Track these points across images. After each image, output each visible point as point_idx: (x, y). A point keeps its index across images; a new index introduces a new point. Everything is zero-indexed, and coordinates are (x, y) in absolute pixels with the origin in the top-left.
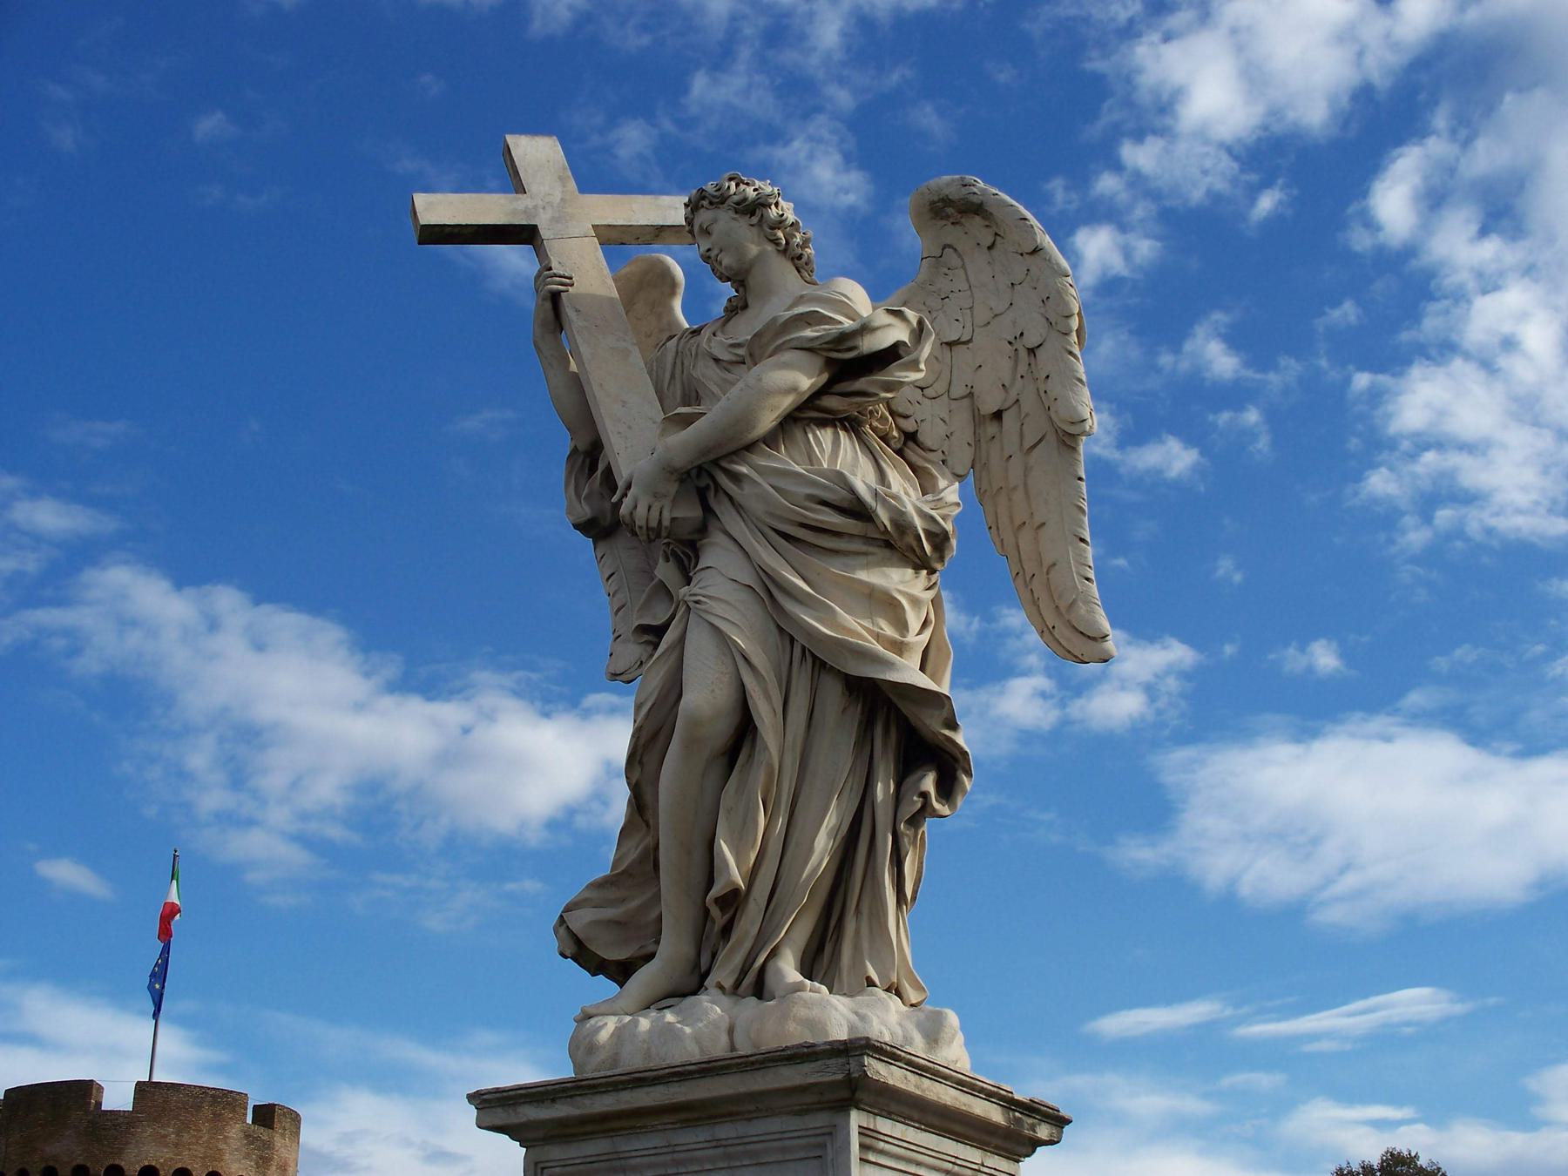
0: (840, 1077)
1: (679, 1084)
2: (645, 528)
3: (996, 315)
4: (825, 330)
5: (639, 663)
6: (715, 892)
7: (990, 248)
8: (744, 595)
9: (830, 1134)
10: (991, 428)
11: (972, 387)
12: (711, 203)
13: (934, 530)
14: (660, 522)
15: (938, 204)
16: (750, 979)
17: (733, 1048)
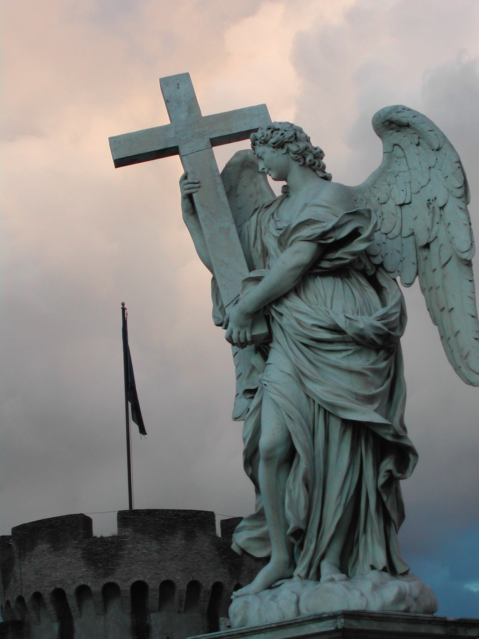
0: (333, 628)
5: (247, 410)
6: (289, 531)
10: (425, 253)
11: (413, 230)
12: (260, 143)
15: (386, 123)
17: (298, 612)
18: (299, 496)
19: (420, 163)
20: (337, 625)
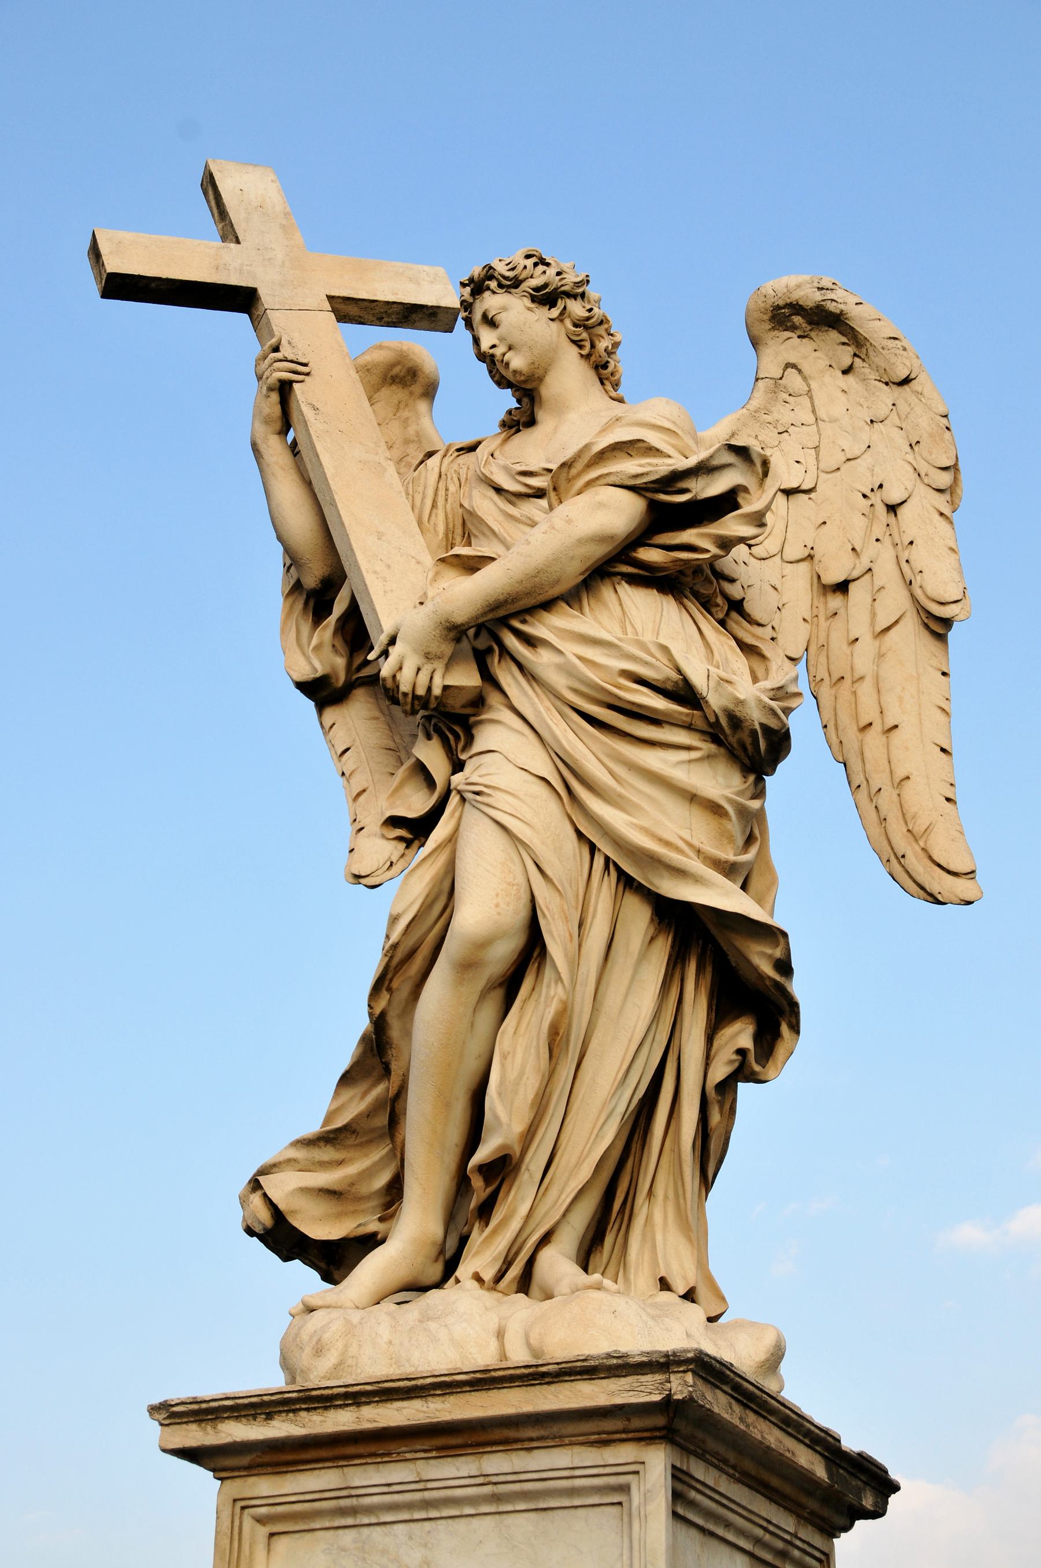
0: (657, 1398)
1: (441, 1398)
2: (410, 696)
3: (849, 460)
4: (650, 464)
5: (388, 863)
9: (637, 1473)
10: (835, 602)
11: (812, 548)
13: (772, 726)
14: (429, 689)
15: (783, 311)
16: (515, 1271)
17: (504, 1356)
18: (521, 1074)
19: (848, 410)
20: (670, 1391)
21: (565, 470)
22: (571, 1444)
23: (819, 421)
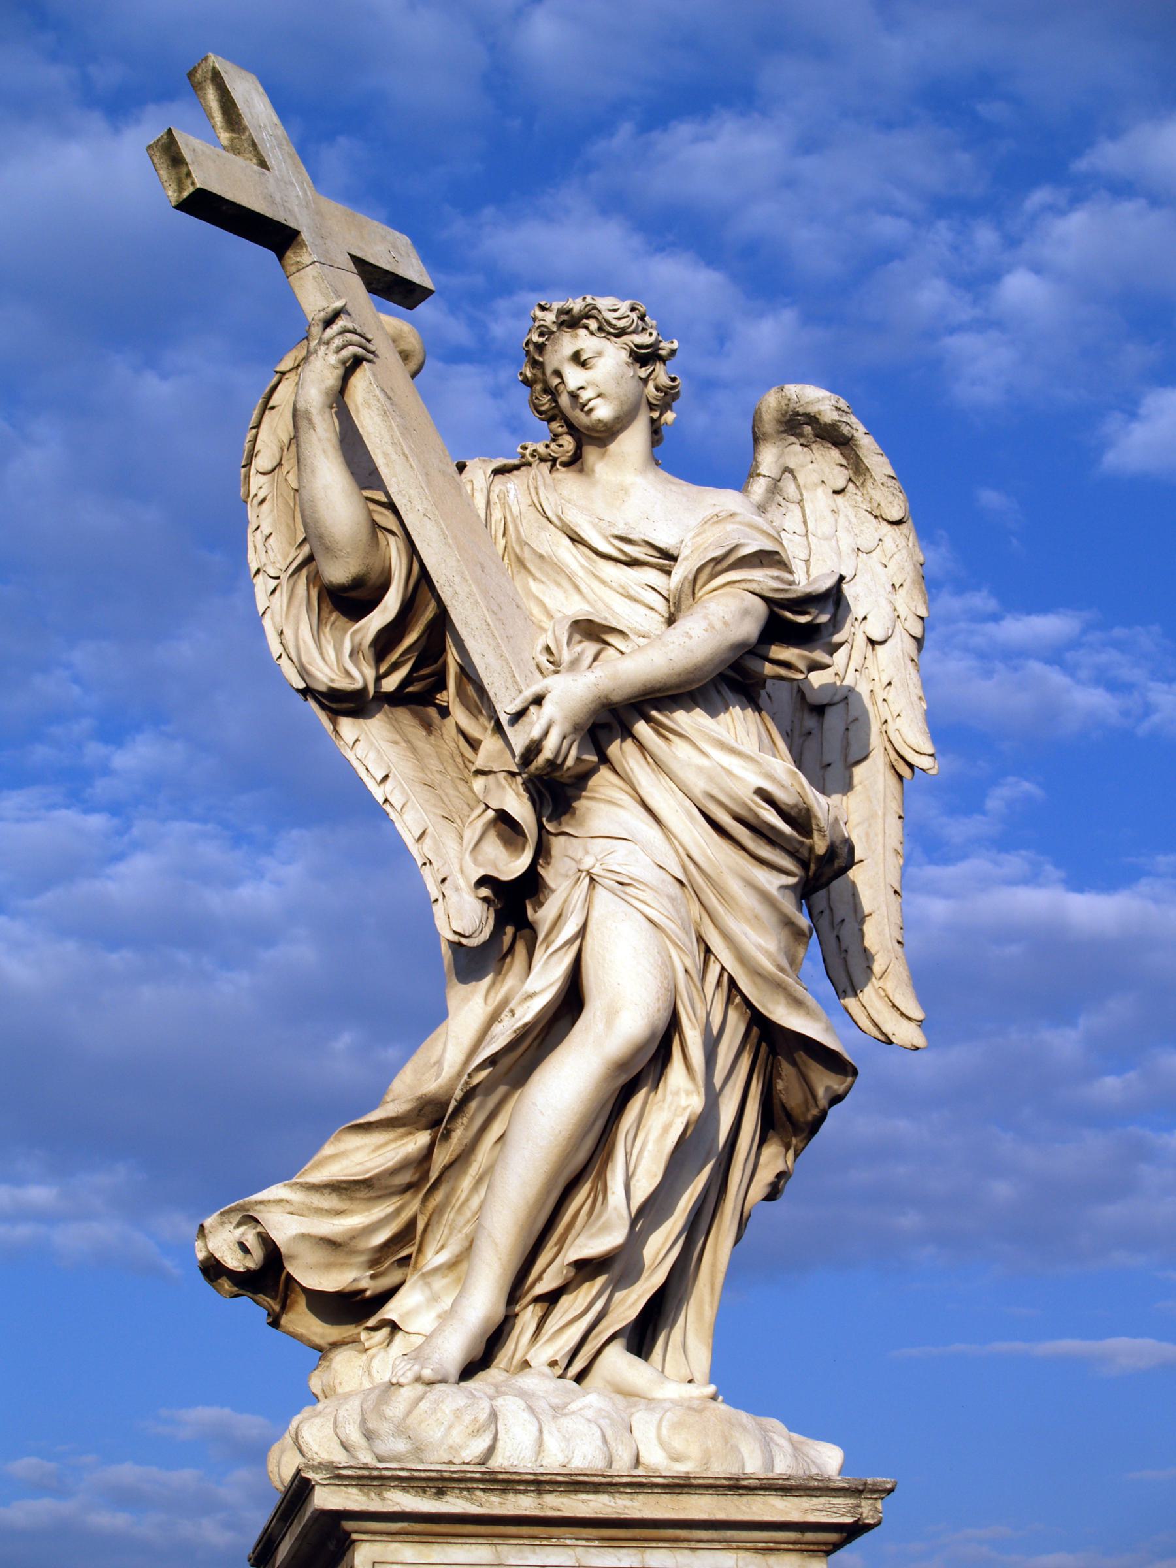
1: (629, 1496)
7: (836, 492)
8: (675, 889)
10: (810, 722)
12: (600, 329)
15: (799, 418)
20: (861, 1514)
21: (712, 564)
22: (738, 1548)
23: (809, 534)
